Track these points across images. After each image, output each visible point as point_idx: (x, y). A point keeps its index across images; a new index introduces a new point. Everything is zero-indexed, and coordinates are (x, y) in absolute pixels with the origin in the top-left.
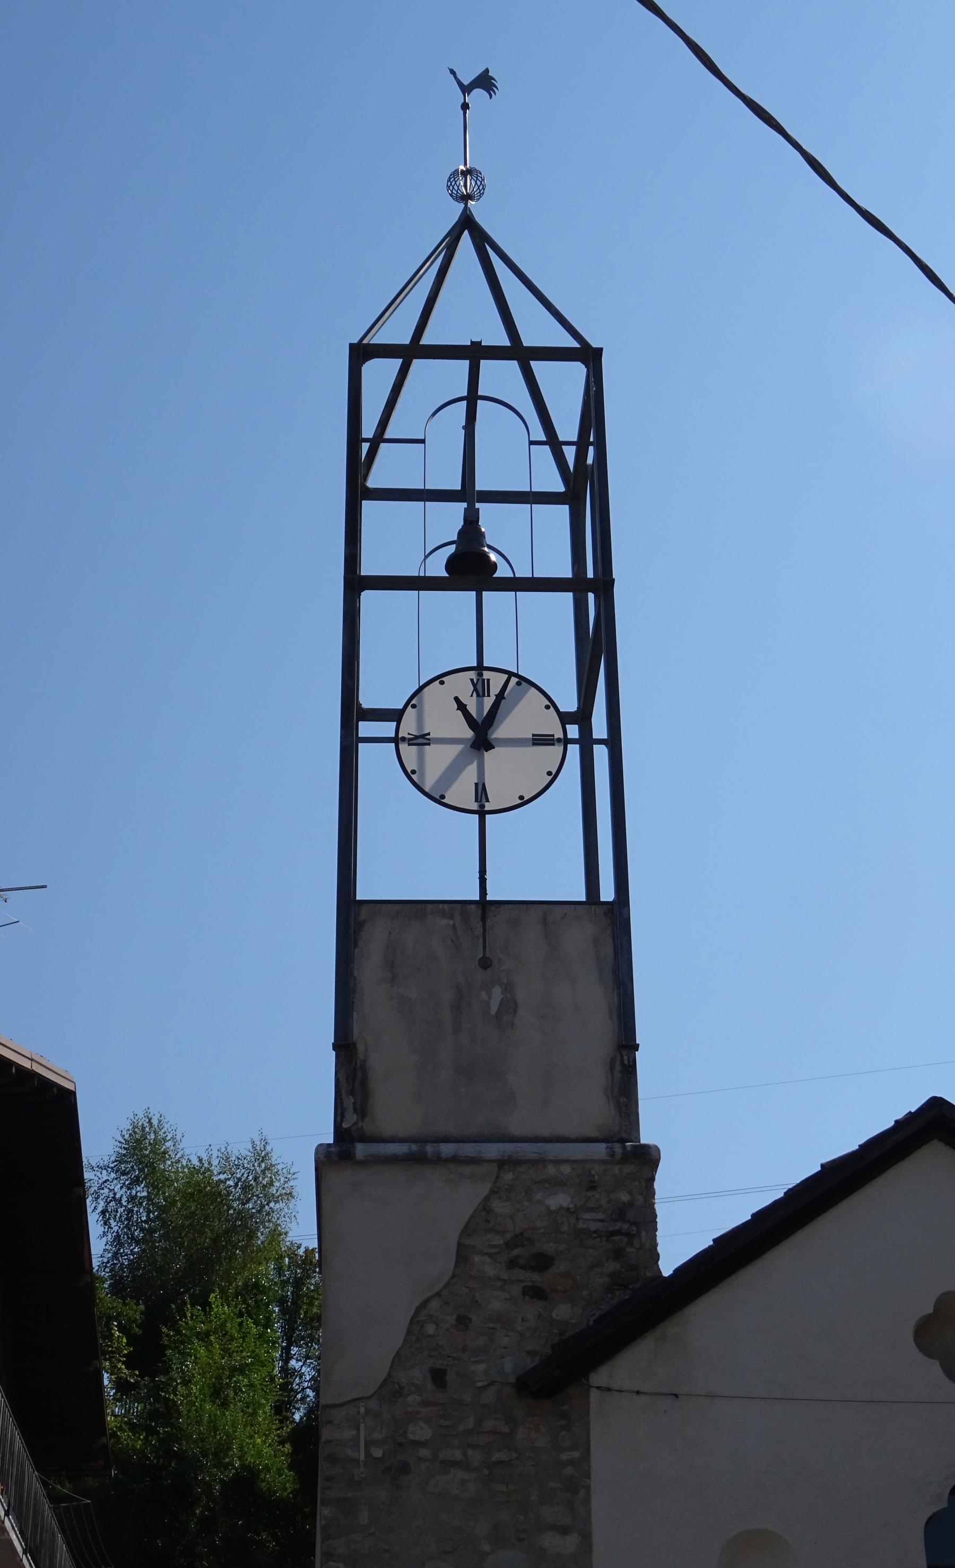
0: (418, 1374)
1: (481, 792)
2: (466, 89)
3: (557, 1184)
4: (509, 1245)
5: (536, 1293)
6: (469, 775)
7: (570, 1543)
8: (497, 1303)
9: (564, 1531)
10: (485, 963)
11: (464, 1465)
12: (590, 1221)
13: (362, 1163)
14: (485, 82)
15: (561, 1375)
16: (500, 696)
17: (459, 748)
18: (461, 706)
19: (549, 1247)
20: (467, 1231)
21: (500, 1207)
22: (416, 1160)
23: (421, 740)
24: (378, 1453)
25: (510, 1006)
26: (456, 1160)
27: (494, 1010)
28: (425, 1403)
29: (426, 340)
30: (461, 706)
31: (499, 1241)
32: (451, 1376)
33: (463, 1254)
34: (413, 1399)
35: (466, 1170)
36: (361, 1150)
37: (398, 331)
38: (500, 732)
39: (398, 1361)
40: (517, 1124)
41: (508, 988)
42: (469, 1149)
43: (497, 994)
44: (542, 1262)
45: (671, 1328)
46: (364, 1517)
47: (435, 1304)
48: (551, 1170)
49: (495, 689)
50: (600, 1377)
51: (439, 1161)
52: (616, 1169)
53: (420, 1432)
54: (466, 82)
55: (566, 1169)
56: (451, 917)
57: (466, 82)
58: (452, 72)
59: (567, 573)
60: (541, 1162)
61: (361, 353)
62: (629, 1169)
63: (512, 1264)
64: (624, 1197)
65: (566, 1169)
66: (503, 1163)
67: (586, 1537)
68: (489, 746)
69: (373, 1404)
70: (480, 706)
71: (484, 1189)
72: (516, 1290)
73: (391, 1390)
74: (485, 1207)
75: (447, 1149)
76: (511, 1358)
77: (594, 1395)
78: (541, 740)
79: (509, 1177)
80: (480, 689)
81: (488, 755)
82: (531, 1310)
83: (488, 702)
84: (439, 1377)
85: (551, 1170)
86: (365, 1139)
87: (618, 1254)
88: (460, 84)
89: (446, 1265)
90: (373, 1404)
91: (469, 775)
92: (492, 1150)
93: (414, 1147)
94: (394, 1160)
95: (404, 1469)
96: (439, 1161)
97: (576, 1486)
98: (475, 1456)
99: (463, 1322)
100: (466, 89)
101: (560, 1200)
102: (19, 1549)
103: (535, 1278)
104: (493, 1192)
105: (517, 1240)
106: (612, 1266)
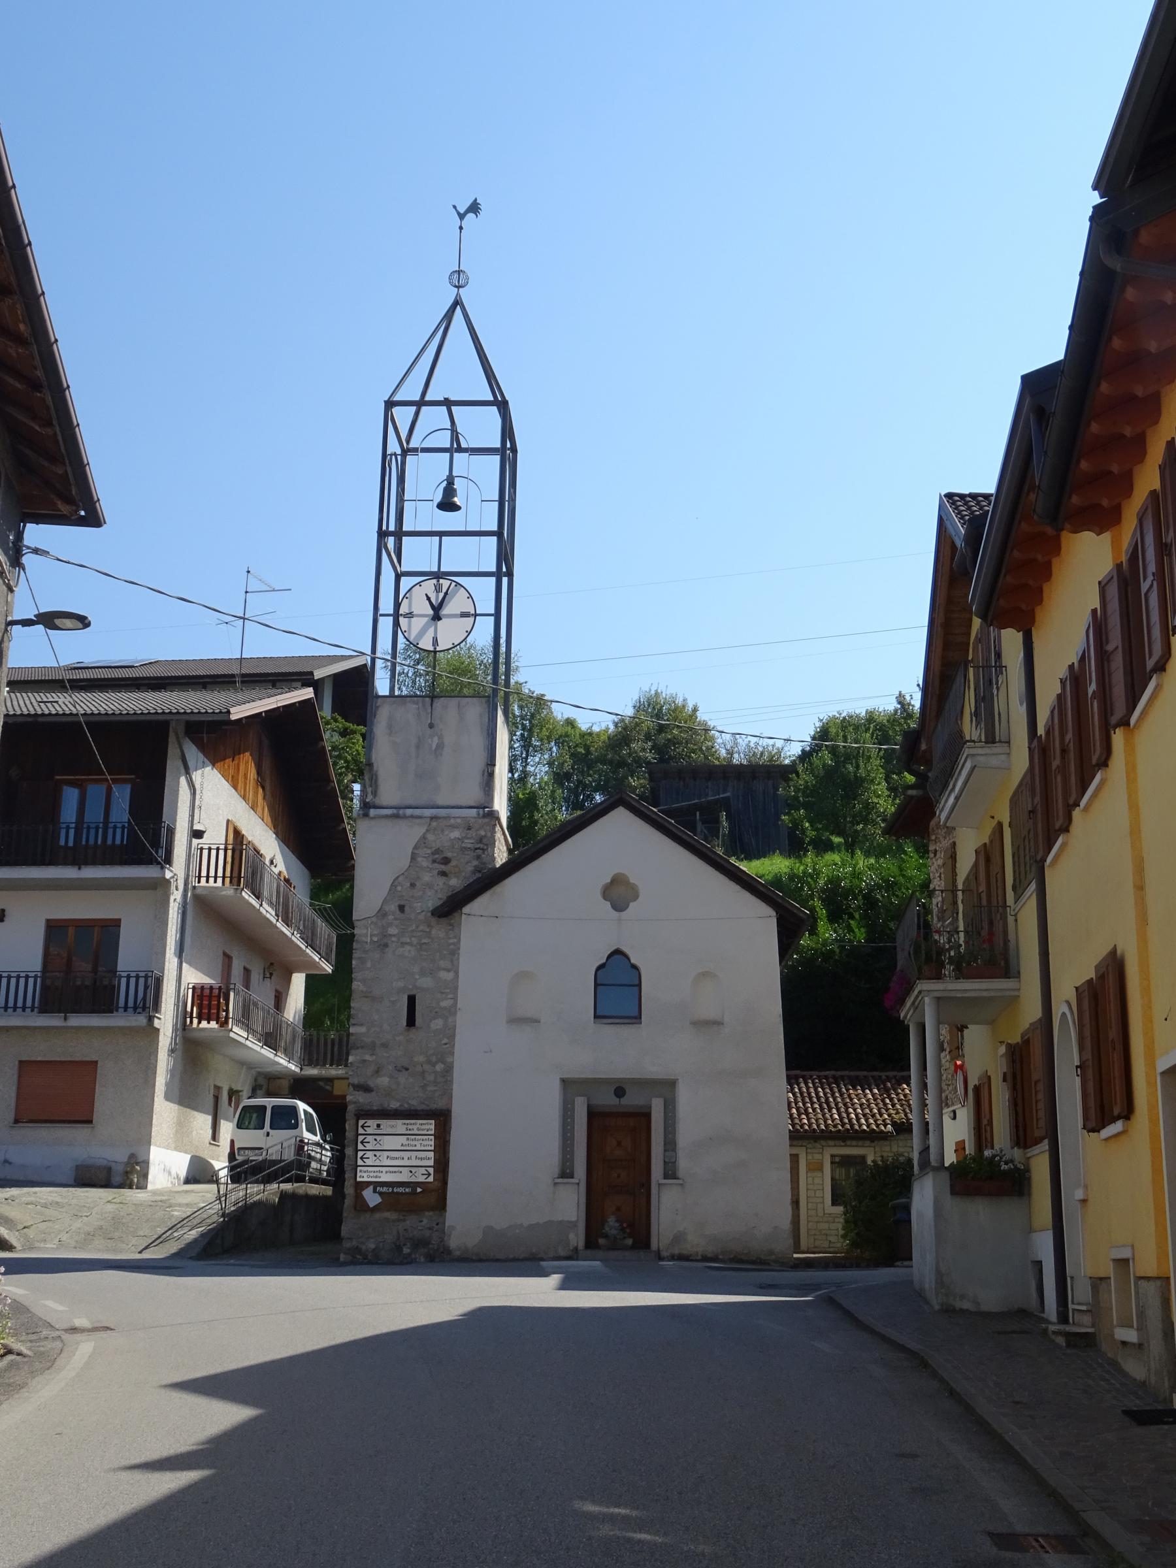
0: (393, 907)
1: (435, 642)
2: (462, 216)
3: (454, 827)
4: (433, 854)
5: (443, 874)
6: (430, 634)
7: (451, 975)
8: (427, 877)
9: (448, 970)
10: (431, 726)
11: (410, 944)
12: (468, 843)
13: (374, 818)
14: (474, 208)
15: (450, 908)
16: (446, 593)
17: (426, 619)
18: (429, 599)
19: (449, 855)
20: (416, 847)
21: (430, 837)
22: (396, 816)
23: (410, 615)
24: (375, 939)
25: (440, 746)
26: (412, 817)
27: (434, 746)
28: (395, 919)
29: (427, 398)
30: (429, 599)
31: (429, 851)
32: (406, 909)
33: (414, 857)
34: (391, 917)
35: (418, 821)
36: (372, 812)
37: (411, 391)
38: (445, 611)
39: (385, 902)
40: (440, 801)
41: (441, 737)
42: (417, 812)
43: (436, 740)
44: (446, 861)
45: (498, 889)
46: (369, 965)
47: (401, 879)
48: (452, 821)
49: (444, 590)
50: (466, 910)
51: (405, 817)
52: (480, 821)
53: (393, 931)
54: (462, 212)
55: (459, 821)
56: (417, 703)
57: (462, 212)
58: (455, 207)
59: (493, 579)
60: (448, 818)
61: (390, 404)
62: (486, 820)
63: (434, 861)
64: (483, 833)
65: (459, 821)
66: (432, 818)
67: (457, 973)
68: (439, 619)
69: (374, 919)
70: (437, 597)
71: (423, 830)
72: (436, 872)
73: (382, 913)
74: (424, 837)
75: (409, 812)
76: (433, 899)
77: (464, 916)
78: (465, 615)
79: (434, 824)
80: (438, 589)
81: (439, 623)
82: (441, 881)
83: (441, 595)
84: (402, 908)
85: (452, 821)
86: (376, 807)
87: (478, 857)
88: (459, 213)
89: (407, 862)
90: (374, 919)
91: (430, 634)
92: (428, 813)
93: (395, 811)
94: (387, 817)
95: (386, 945)
96: (405, 817)
97: (454, 953)
98: (415, 941)
99: (413, 885)
100: (462, 216)
101: (456, 834)
102: (271, 1056)
103: (443, 868)
104: (427, 831)
105: (437, 851)
106: (475, 863)
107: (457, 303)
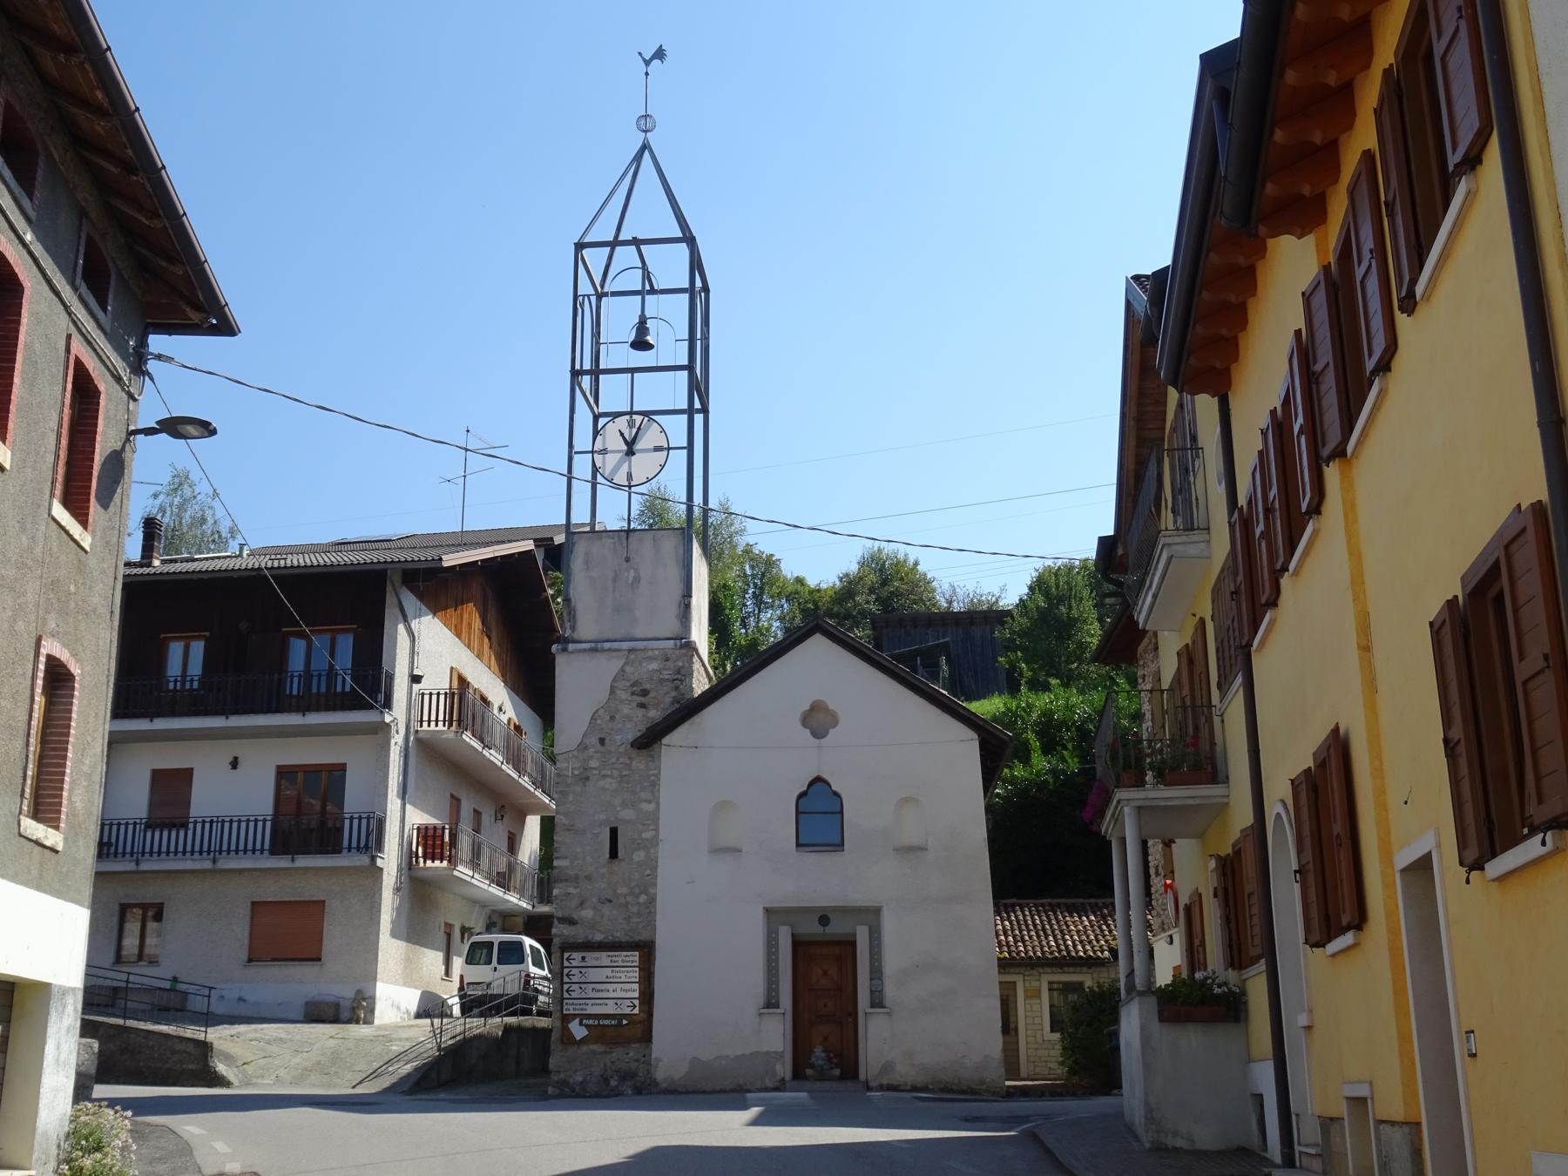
0: (594, 740)
1: (630, 477)
2: (647, 63)
3: (652, 659)
4: (633, 685)
5: (642, 706)
7: (651, 807)
8: (626, 710)
12: (666, 675)
14: (660, 54)
15: (650, 739)
19: (647, 686)
20: (614, 680)
21: (629, 669)
22: (595, 650)
23: (604, 452)
25: (637, 579)
33: (613, 690)
38: (638, 446)
41: (637, 570)
42: (616, 645)
43: (632, 573)
44: (645, 693)
45: (697, 719)
50: (665, 741)
51: (603, 650)
53: (593, 763)
59: (685, 417)
60: (645, 650)
61: (580, 246)
66: (630, 651)
67: (658, 804)
73: (583, 747)
74: (622, 670)
75: (607, 645)
78: (658, 449)
80: (631, 424)
82: (640, 712)
84: (602, 741)
87: (677, 688)
92: (626, 645)
94: (585, 650)
95: (587, 778)
96: (603, 650)
97: (655, 785)
99: (612, 718)
100: (647, 63)
101: (654, 666)
103: (642, 699)
105: (634, 684)
106: (674, 694)
107: (645, 147)
